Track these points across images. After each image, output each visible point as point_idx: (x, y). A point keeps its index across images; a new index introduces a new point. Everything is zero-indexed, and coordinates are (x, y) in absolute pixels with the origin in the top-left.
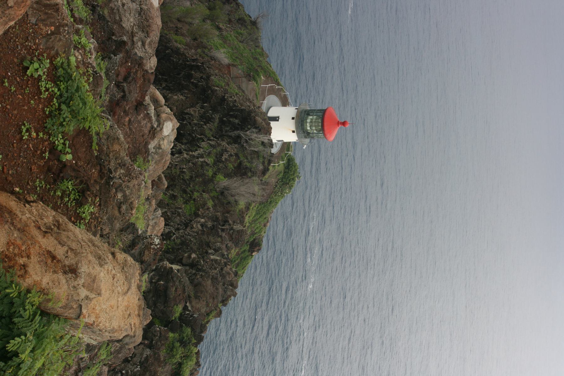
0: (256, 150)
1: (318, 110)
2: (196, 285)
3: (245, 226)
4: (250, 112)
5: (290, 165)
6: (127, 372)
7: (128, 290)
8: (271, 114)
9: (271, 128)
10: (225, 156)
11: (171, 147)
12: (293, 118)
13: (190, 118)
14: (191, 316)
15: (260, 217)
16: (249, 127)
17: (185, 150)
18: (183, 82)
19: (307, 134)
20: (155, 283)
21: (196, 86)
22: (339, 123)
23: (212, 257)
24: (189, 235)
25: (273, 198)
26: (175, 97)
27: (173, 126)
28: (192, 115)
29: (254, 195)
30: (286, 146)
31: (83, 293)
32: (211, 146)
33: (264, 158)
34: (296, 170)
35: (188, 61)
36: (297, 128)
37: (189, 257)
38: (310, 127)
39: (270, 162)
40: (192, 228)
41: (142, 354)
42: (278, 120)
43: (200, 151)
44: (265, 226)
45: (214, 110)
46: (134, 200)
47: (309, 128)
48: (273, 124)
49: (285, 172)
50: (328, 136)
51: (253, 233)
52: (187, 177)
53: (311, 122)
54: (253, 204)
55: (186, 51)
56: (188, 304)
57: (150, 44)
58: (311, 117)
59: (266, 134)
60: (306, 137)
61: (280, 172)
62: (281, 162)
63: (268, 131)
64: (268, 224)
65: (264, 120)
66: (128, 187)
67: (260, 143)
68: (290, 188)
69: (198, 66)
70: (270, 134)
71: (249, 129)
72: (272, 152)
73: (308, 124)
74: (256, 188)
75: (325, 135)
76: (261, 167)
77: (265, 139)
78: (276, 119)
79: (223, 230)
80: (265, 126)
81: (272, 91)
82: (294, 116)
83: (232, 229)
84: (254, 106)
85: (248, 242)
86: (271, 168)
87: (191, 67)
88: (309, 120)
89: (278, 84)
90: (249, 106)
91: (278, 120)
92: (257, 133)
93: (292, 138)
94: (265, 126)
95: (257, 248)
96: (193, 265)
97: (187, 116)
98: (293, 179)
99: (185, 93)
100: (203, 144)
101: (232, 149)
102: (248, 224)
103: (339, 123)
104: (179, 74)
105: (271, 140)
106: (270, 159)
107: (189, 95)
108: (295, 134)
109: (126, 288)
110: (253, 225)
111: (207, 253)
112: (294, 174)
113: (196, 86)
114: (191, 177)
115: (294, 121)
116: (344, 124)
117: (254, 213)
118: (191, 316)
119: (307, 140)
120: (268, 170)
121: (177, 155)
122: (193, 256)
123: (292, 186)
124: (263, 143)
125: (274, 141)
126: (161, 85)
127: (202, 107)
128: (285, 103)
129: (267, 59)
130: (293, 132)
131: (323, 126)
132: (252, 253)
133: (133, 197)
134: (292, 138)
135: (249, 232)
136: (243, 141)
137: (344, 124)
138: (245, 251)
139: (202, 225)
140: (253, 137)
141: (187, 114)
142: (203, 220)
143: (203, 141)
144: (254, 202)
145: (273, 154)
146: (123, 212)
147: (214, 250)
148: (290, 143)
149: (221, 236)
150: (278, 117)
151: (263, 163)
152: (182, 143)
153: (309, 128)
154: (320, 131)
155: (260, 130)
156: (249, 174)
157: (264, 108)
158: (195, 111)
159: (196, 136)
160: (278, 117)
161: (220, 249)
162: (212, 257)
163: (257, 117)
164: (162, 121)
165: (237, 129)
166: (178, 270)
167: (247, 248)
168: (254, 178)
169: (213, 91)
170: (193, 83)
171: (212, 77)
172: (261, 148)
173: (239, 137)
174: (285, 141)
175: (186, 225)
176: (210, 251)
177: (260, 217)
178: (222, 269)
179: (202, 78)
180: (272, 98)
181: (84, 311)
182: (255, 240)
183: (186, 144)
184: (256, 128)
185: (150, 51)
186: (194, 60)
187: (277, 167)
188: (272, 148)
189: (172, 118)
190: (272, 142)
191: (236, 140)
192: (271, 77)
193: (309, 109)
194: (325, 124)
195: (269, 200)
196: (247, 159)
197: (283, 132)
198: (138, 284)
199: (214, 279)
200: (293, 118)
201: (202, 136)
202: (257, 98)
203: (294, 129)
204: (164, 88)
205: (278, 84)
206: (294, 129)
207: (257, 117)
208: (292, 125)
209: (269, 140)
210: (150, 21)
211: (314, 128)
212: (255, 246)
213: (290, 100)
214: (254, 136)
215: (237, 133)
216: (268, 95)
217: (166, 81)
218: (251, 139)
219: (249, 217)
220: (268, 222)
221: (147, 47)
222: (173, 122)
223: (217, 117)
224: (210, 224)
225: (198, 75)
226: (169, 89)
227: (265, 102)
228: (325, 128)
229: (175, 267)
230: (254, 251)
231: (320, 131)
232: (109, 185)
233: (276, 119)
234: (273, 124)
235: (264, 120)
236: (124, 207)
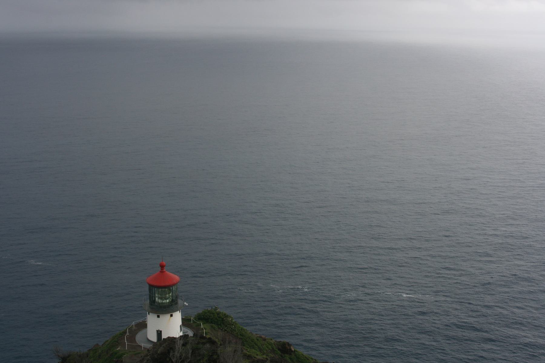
0: (191, 351)
1: (150, 292)
3: (266, 358)
5: (205, 317)
9: (169, 337)
12: (158, 317)
15: (256, 345)
16: (168, 359)
22: (162, 272)
25: (237, 333)
29: (235, 351)
30: (186, 322)
33: (198, 343)
34: (209, 311)
36: (168, 313)
38: (166, 299)
39: (202, 337)
44: (265, 340)
47: (168, 301)
48: (164, 336)
49: (212, 322)
50: (175, 281)
51: (273, 351)
53: (161, 298)
54: (245, 351)
58: (157, 299)
59: (175, 342)
60: (177, 303)
61: (212, 327)
62: (202, 326)
63: (171, 340)
64: (263, 336)
65: (161, 345)
67: (183, 347)
68: (226, 316)
70: (175, 338)
71: (170, 359)
73: (164, 302)
74: (229, 349)
75: (174, 285)
76: (208, 346)
78: (159, 333)
80: (167, 343)
81: (132, 338)
84: (147, 355)
85: (281, 356)
86: (208, 336)
88: (160, 301)
89: (125, 332)
90: (148, 360)
91: (161, 331)
92: (174, 352)
93: (178, 317)
94: (167, 343)
95: (287, 346)
98: (218, 314)
102: (265, 356)
103: (162, 272)
108: (174, 314)
110: (265, 352)
112: (213, 313)
115: (161, 316)
116: (162, 266)
117: (253, 350)
119: (180, 301)
120: (210, 338)
123: (225, 314)
124: (184, 345)
125: (181, 334)
128: (143, 326)
129: (101, 344)
130: (171, 316)
131: (165, 287)
132: (292, 351)
134: (178, 317)
135: (272, 355)
137: (162, 266)
138: (290, 359)
140: (178, 355)
144: (242, 351)
145: (194, 335)
148: (182, 319)
150: (158, 331)
151: (204, 344)
153: (168, 301)
154: (170, 290)
155: (171, 348)
156: (215, 357)
157: (149, 346)
160: (158, 331)
163: (159, 352)
167: (287, 357)
168: (219, 352)
172: (189, 346)
174: (180, 323)
177: (256, 345)
180: (139, 337)
182: (279, 349)
184: (169, 353)
187: (207, 331)
188: (188, 335)
192: (118, 340)
193: (148, 301)
194: (163, 284)
195: (240, 337)
196: (200, 360)
197: (173, 326)
200: (158, 317)
202: (139, 353)
203: (169, 315)
205: (125, 332)
206: (169, 315)
207: (159, 352)
208: (166, 318)
209: (180, 339)
211: (167, 295)
212: (285, 349)
213: (141, 320)
214: (177, 354)
216: (136, 342)
218: (180, 356)
219: (257, 355)
220: (261, 337)
227: (143, 345)
228: (167, 284)
230: (290, 349)
231: (170, 290)
233: (159, 333)
234: (164, 336)
235: (161, 345)
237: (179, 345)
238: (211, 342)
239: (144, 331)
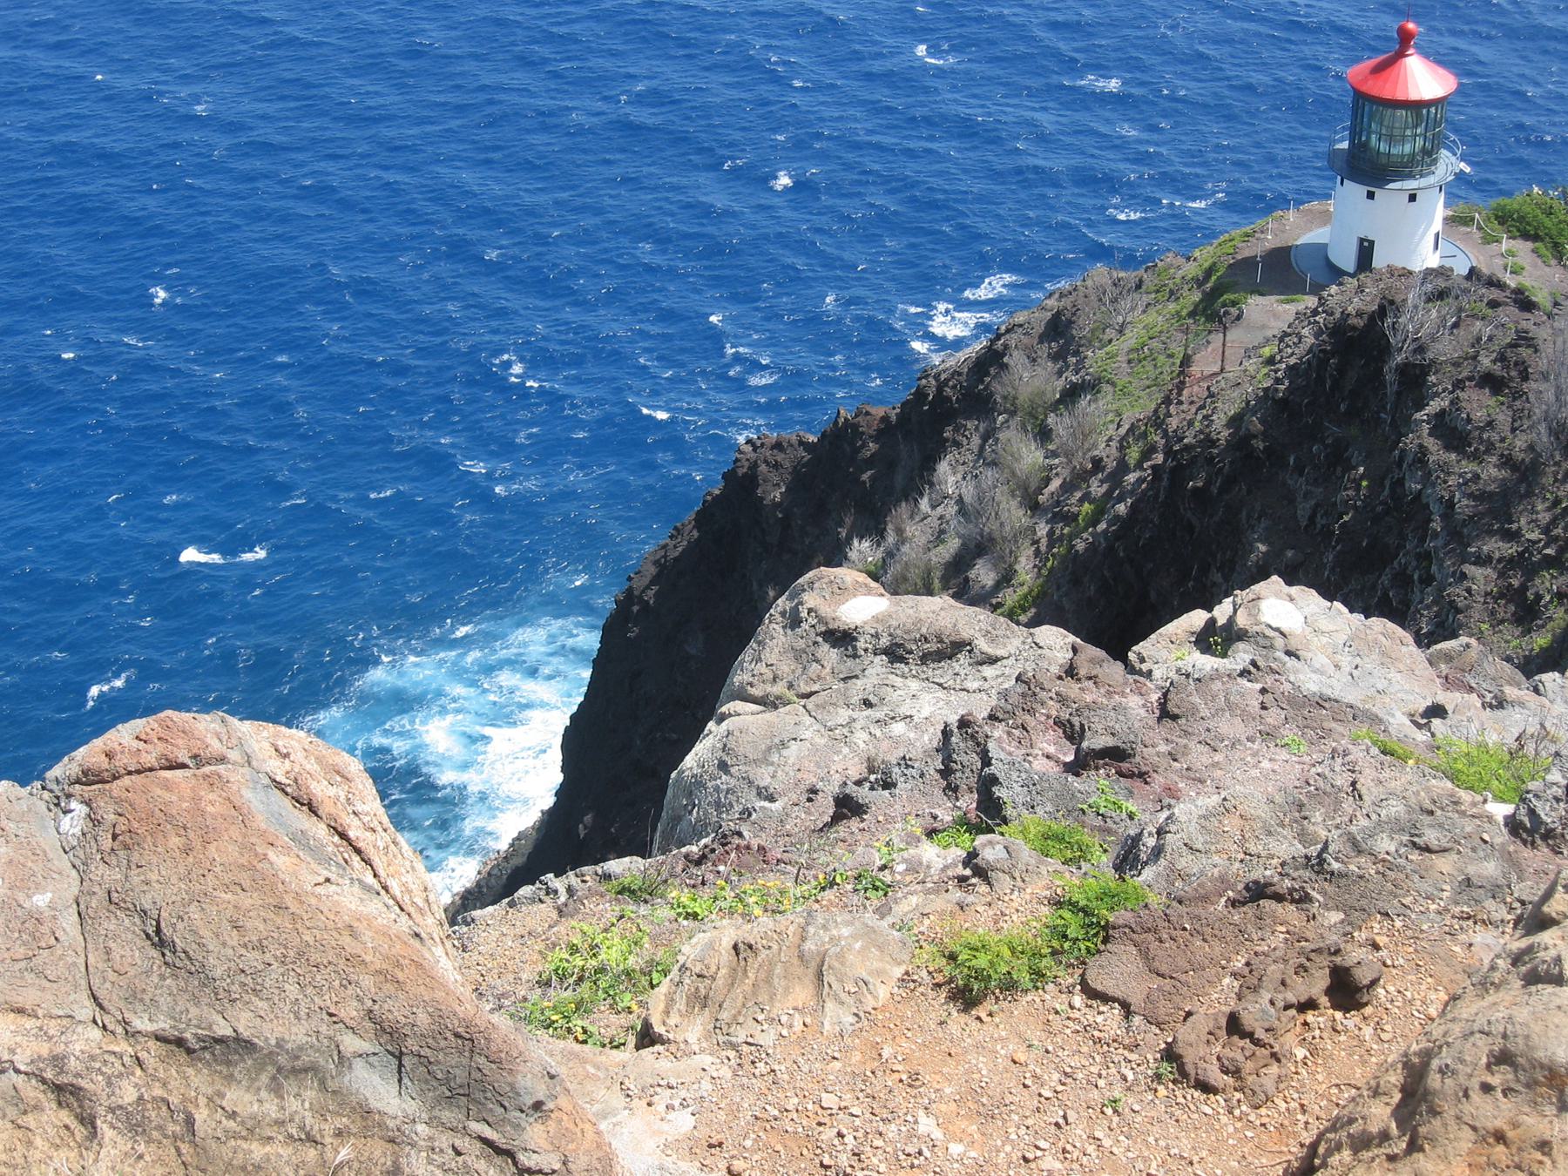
11: (1345, 610)
12: (1371, 195)
13: (1326, 513)
17: (1422, 540)
18: (1216, 519)
27: (1277, 595)
28: (1317, 505)
35: (1156, 496)
42: (1372, 243)
46: (1428, 790)
57: (993, 640)
66: (1379, 803)
72: (1465, 272)
76: (1509, 315)
82: (1362, 190)
86: (1511, 281)
88: (1383, 147)
91: (1372, 243)
97: (1320, 521)
99: (1249, 517)
105: (1429, 272)
107: (1258, 507)
120: (1519, 291)
121: (1434, 568)
126: (1214, 584)
133: (1417, 794)
136: (1418, 359)
141: (1312, 519)
146: (1444, 843)
150: (1362, 240)
152: (1401, 547)
158: (1307, 495)
159: (1381, 503)
160: (1362, 240)
164: (1256, 628)
170: (1222, 490)
173: (1404, 370)
183: (1403, 537)
185: (1016, 642)
189: (1251, 596)
190: (1433, 270)
200: (1371, 195)
201: (1387, 483)
204: (1226, 578)
210: (924, 630)
221: (1000, 652)
222: (1263, 594)
223: (1334, 430)
232: (1341, 875)
234: (1379, 261)
236: (1431, 837)
238: (1525, 304)
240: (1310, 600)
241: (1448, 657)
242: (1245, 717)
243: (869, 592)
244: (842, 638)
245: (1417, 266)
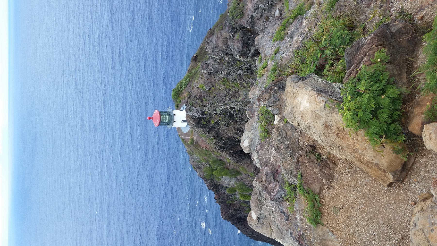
2: (226, 44)
4: (196, 126)
6: (266, 5)
7: (293, 108)
8: (186, 124)
10: (209, 106)
14: (231, 32)
19: (168, 113)
20: (248, 50)
21: (221, 139)
23: (218, 57)
24: (228, 69)
26: (232, 134)
27: (243, 144)
30: (178, 108)
31: (322, 114)
32: (216, 111)
37: (229, 59)
40: (226, 72)
41: (257, 13)
43: (221, 108)
45: (213, 127)
47: (167, 116)
52: (228, 96)
53: (166, 119)
55: (226, 154)
56: (232, 37)
57: (256, 193)
65: (189, 122)
69: (221, 148)
70: (187, 115)
73: (168, 118)
77: (190, 114)
78: (183, 121)
79: (211, 70)
83: (207, 70)
87: (224, 148)
88: (167, 120)
93: (176, 112)
96: (227, 54)
100: (219, 111)
101: (205, 109)
104: (230, 145)
105: (186, 112)
106: (187, 103)
109: (295, 108)
111: (220, 60)
113: (221, 139)
114: (226, 96)
118: (231, 32)
122: (227, 59)
125: (185, 111)
127: (219, 129)
128: (179, 128)
139: (222, 73)
141: (226, 126)
142: (221, 76)
143: (219, 113)
147: (216, 61)
149: (212, 67)
157: (189, 127)
161: (214, 61)
162: (218, 57)
165: (203, 118)
166: (236, 56)
169: (214, 136)
171: (214, 143)
173: (202, 115)
175: (229, 74)
176: (218, 60)
178: (213, 51)
179: (219, 143)
181: (323, 105)
183: (228, 112)
184: (194, 118)
186: (222, 151)
191: (203, 113)
197: (180, 116)
198: (286, 107)
199: (217, 47)
208: (176, 118)
215: (203, 117)
217: (236, 142)
224: (218, 74)
225: (221, 144)
226: (234, 138)
229: (238, 57)
233: (183, 121)
234: (186, 119)
237: (190, 114)
239: (182, 129)
240: (243, 138)
241: (249, 115)
242: (265, 153)
243: (251, 214)
244: (259, 219)
245: (186, 114)
